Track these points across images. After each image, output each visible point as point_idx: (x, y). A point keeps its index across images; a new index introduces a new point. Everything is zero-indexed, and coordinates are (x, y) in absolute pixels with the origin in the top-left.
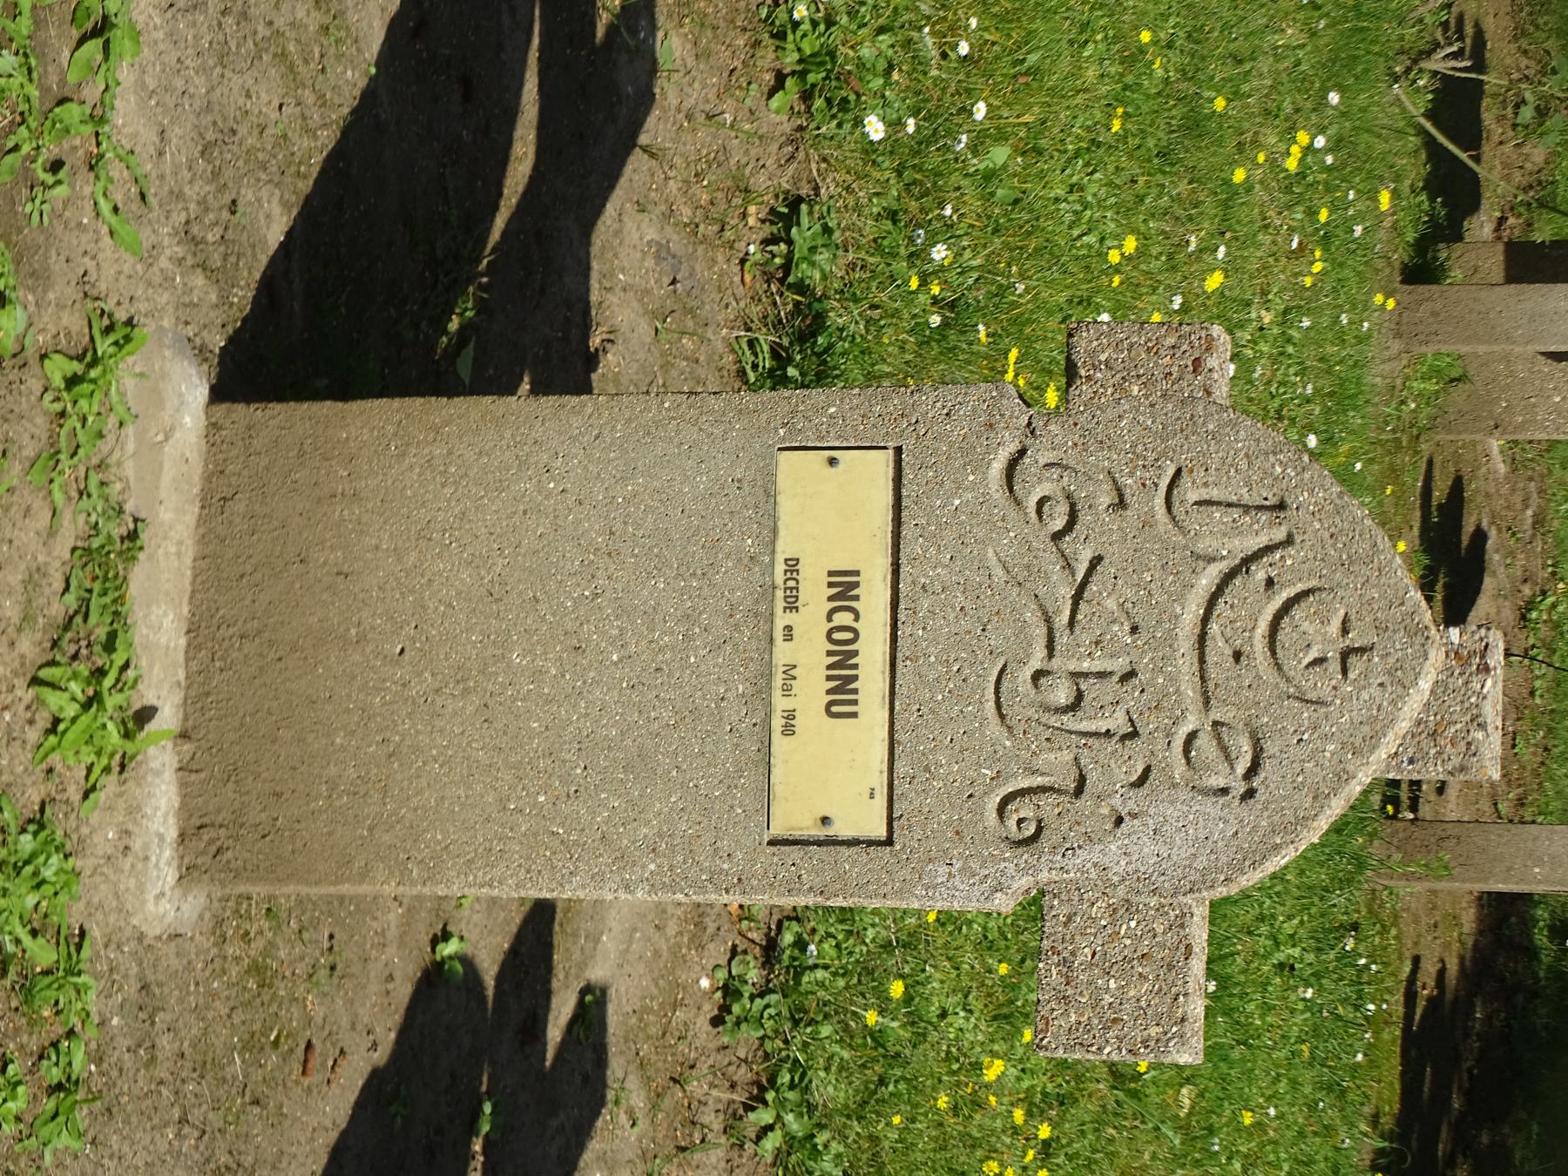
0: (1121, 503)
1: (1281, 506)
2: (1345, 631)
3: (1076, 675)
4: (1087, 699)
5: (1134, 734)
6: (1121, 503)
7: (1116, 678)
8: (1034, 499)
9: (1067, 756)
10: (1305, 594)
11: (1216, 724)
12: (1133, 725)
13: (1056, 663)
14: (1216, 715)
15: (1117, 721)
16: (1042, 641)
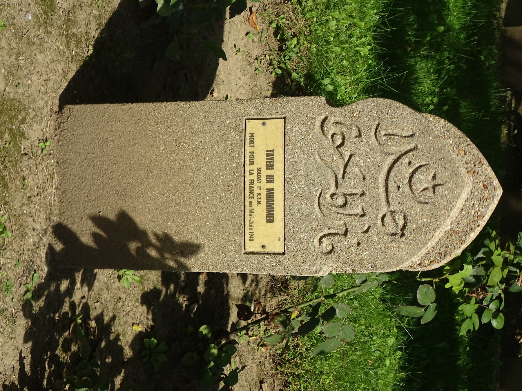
0: (360, 135)
1: (412, 135)
2: (434, 177)
3: (345, 195)
4: (349, 203)
5: (364, 215)
6: (360, 135)
7: (359, 196)
8: (331, 132)
9: (342, 222)
10: (421, 166)
11: (392, 212)
12: (363, 211)
13: (339, 191)
14: (392, 208)
15: (359, 211)
16: (333, 184)
